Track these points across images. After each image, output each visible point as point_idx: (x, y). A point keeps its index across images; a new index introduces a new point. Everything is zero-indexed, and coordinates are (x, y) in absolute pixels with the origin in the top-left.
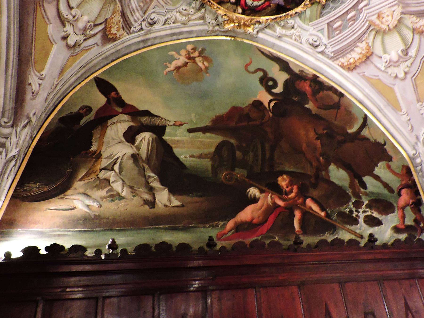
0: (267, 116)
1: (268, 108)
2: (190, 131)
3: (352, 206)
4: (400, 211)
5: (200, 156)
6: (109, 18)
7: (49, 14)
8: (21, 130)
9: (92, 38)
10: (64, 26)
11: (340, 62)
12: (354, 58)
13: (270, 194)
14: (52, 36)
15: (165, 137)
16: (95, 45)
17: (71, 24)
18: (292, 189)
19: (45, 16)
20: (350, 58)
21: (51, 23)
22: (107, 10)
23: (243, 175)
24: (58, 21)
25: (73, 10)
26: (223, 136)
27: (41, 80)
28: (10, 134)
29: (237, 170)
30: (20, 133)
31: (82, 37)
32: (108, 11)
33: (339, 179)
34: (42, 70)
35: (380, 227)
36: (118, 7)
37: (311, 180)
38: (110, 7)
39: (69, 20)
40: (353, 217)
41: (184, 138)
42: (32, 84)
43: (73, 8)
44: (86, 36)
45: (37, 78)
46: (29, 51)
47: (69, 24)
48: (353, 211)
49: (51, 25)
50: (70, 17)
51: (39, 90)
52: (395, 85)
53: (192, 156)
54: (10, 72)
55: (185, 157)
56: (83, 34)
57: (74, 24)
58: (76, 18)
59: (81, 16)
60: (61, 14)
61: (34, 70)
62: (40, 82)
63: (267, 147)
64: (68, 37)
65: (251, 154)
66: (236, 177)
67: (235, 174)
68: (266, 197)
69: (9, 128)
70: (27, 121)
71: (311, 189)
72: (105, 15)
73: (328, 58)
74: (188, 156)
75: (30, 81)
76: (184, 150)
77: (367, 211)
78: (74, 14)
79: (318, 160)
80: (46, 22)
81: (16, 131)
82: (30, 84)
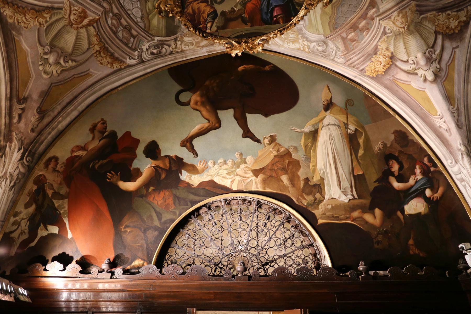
6: (436, 28)
7: (403, 79)
8: (463, 162)
9: (443, 53)
10: (417, 74)
14: (419, 87)
16: (454, 50)
17: (418, 69)
19: (404, 82)
21: (410, 82)
22: (426, 29)
24: (412, 76)
25: (409, 61)
27: (442, 118)
28: (460, 169)
30: (464, 165)
31: (435, 65)
32: (427, 28)
34: (437, 112)
36: (431, 16)
38: (425, 26)
39: (414, 68)
42: (441, 125)
43: (408, 60)
44: (436, 60)
45: (440, 119)
46: (420, 108)
47: (417, 70)
49: (412, 82)
50: (413, 66)
51: (448, 126)
54: (425, 130)
56: (432, 63)
57: (419, 67)
58: (416, 62)
59: (416, 58)
60: (408, 70)
61: (433, 116)
62: (443, 120)
64: (426, 77)
69: (455, 166)
70: (460, 153)
72: (430, 32)
75: (438, 125)
78: (412, 62)
80: (407, 84)
81: (461, 165)
82: (440, 127)
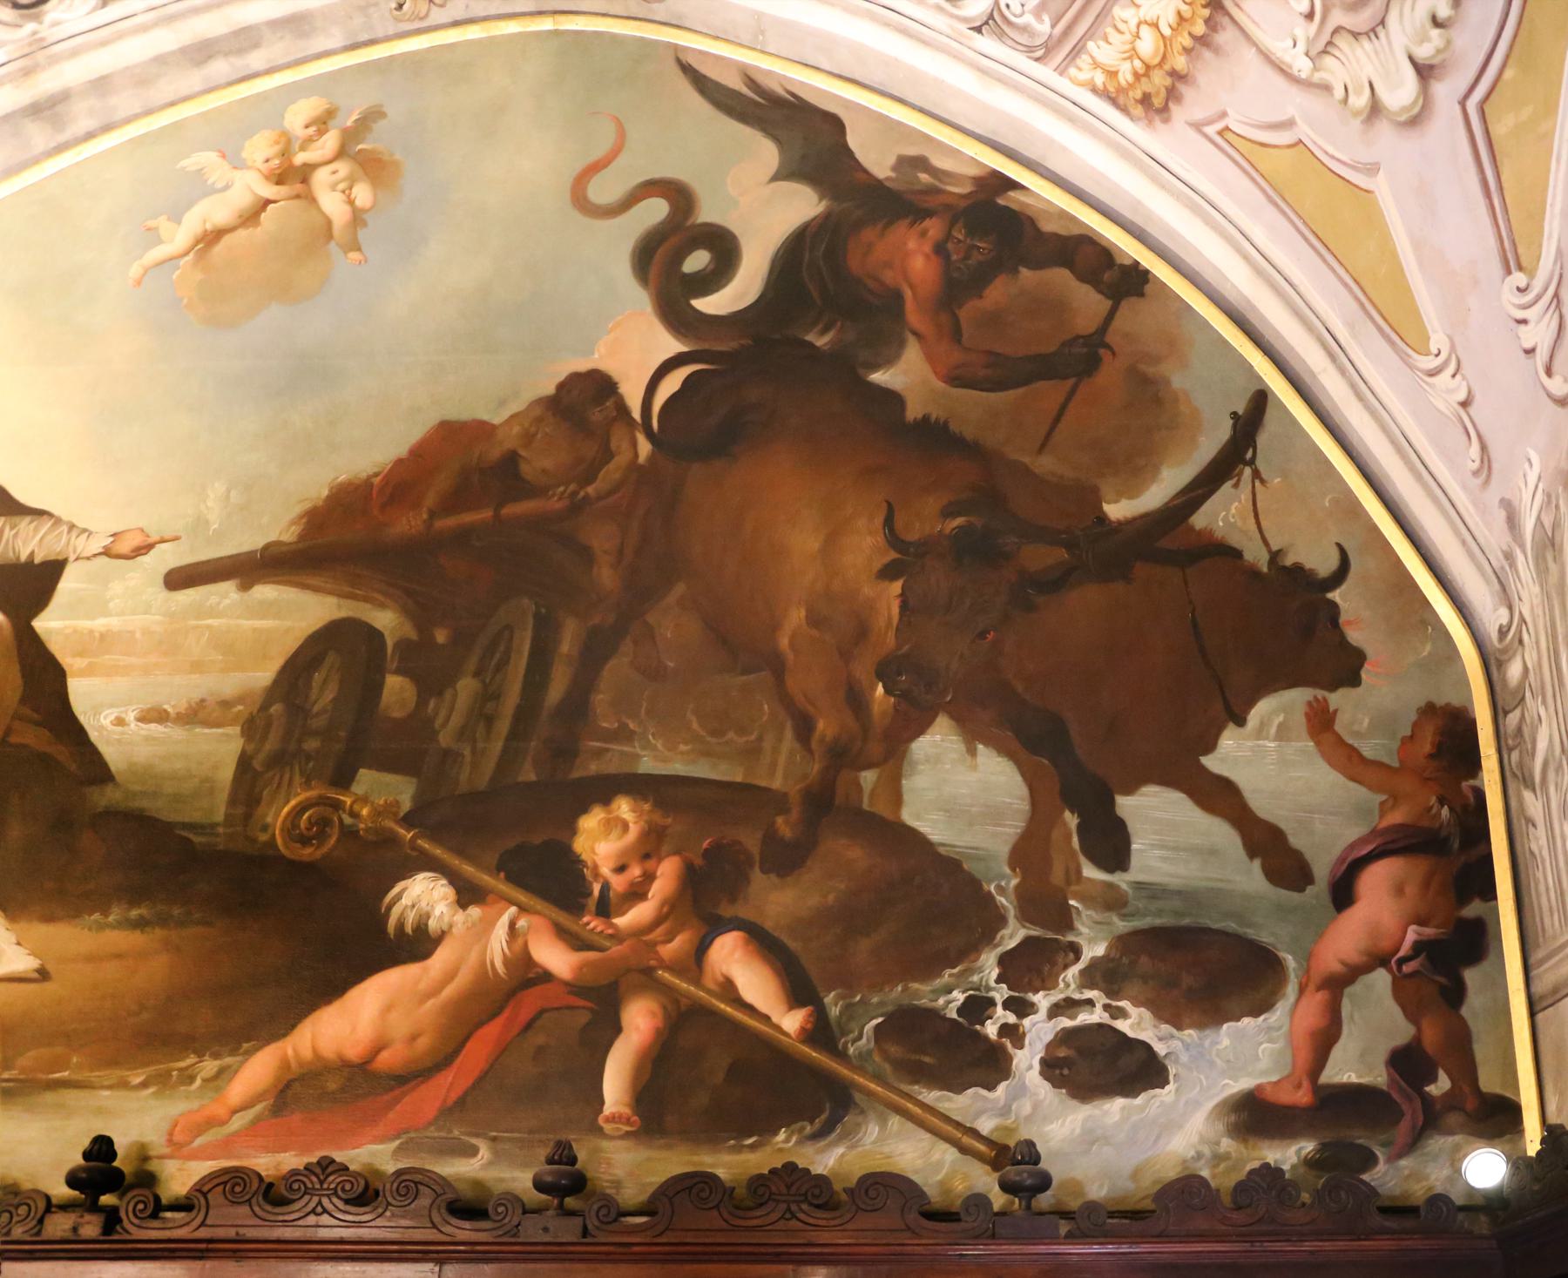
0: (621, 460)
1: (636, 414)
2: (179, 579)
3: (995, 973)
4: (1316, 1001)
5: (195, 715)
11: (1096, 65)
12: (1155, 25)
13: (513, 909)
15: (44, 624)
18: (649, 877)
20: (1133, 23)
23: (390, 809)
26: (340, 595)
29: (367, 780)
33: (952, 810)
35: (1139, 1100)
37: (780, 820)
40: (986, 1038)
41: (137, 622)
48: (991, 1003)
52: (1372, 169)
53: (155, 715)
55: (120, 722)
63: (568, 642)
65: (466, 687)
66: (348, 820)
67: (348, 801)
68: (488, 925)
71: (758, 878)
73: (1029, 49)
74: (131, 716)
76: (121, 684)
77: (1090, 1003)
79: (856, 701)
